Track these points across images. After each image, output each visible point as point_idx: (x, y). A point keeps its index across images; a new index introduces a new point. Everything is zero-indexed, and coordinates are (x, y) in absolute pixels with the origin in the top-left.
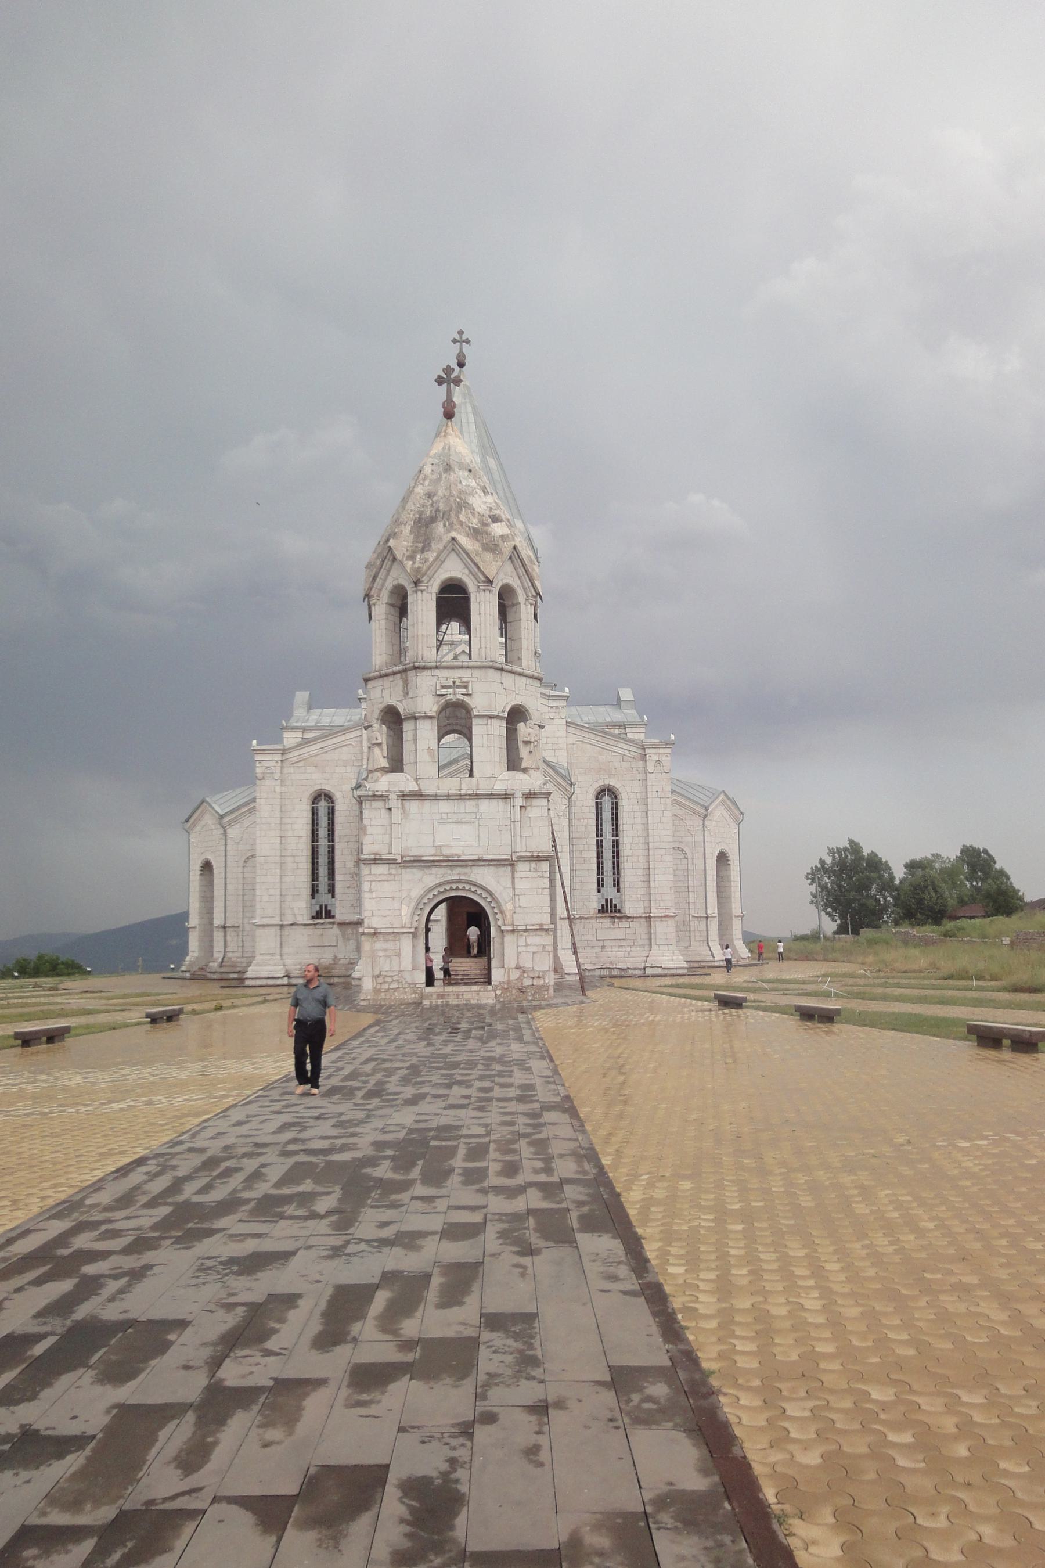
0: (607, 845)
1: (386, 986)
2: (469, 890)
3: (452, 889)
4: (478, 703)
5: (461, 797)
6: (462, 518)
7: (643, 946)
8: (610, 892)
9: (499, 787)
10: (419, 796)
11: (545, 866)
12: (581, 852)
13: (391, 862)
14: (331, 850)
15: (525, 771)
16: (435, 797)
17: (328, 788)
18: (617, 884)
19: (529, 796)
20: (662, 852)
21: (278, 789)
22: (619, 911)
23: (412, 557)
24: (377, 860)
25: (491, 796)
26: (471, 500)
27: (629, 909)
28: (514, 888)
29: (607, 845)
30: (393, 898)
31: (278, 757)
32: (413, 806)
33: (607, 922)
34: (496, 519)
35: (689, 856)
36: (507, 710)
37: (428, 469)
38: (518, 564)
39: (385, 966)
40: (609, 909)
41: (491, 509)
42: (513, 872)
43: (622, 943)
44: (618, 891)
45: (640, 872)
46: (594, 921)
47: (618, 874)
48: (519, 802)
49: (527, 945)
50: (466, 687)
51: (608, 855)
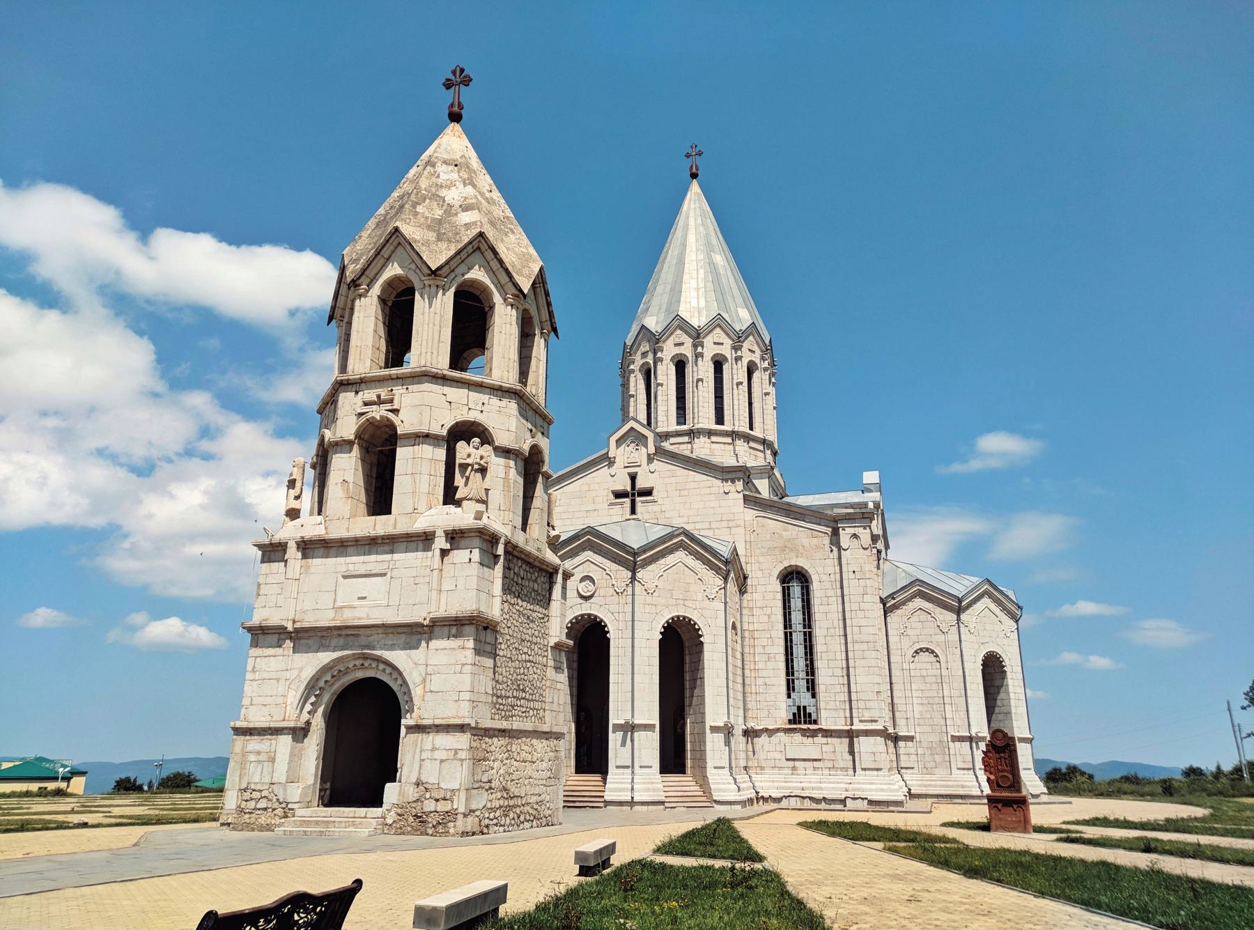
0: (798, 638)
1: (252, 804)
7: (846, 769)
8: (804, 698)
12: (764, 647)
15: (458, 503)
18: (812, 687)
20: (865, 646)
22: (815, 722)
23: (356, 261)
26: (443, 192)
29: (798, 638)
30: (278, 680)
33: (797, 737)
34: (466, 208)
35: (942, 658)
36: (447, 426)
38: (489, 255)
39: (257, 776)
40: (802, 719)
41: (466, 198)
43: (816, 764)
44: (814, 696)
45: (839, 672)
47: (813, 674)
48: (440, 543)
49: (434, 749)
50: (391, 401)
51: (799, 651)
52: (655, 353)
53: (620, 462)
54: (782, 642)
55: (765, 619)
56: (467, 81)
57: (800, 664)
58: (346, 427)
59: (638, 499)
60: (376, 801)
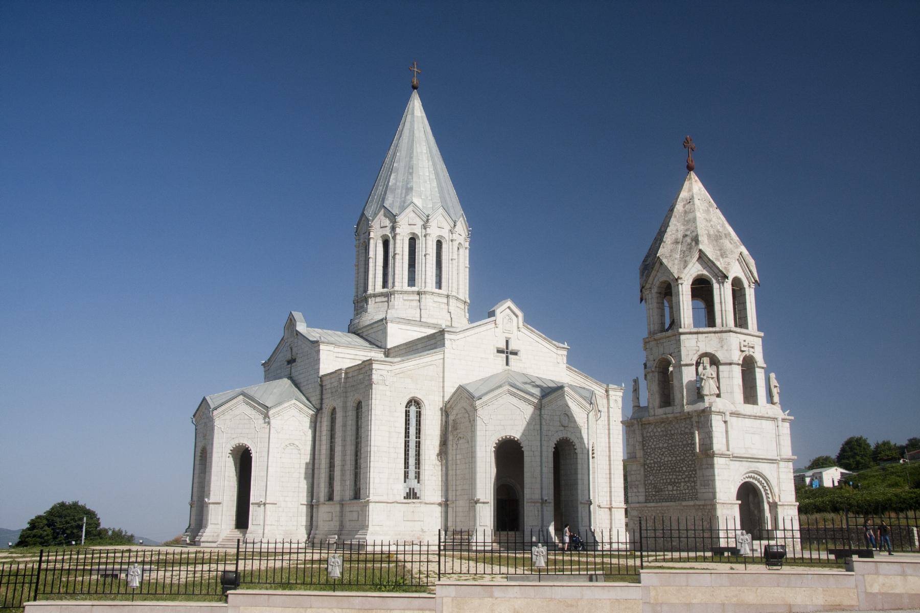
2: (756, 479)
3: (750, 477)
5: (756, 417)
9: (771, 414)
11: (791, 464)
14: (418, 445)
16: (745, 416)
17: (419, 396)
19: (784, 420)
21: (388, 393)
23: (719, 260)
24: (722, 455)
28: (779, 478)
31: (388, 368)
37: (697, 202)
42: (778, 467)
52: (425, 227)
53: (500, 326)
59: (511, 356)
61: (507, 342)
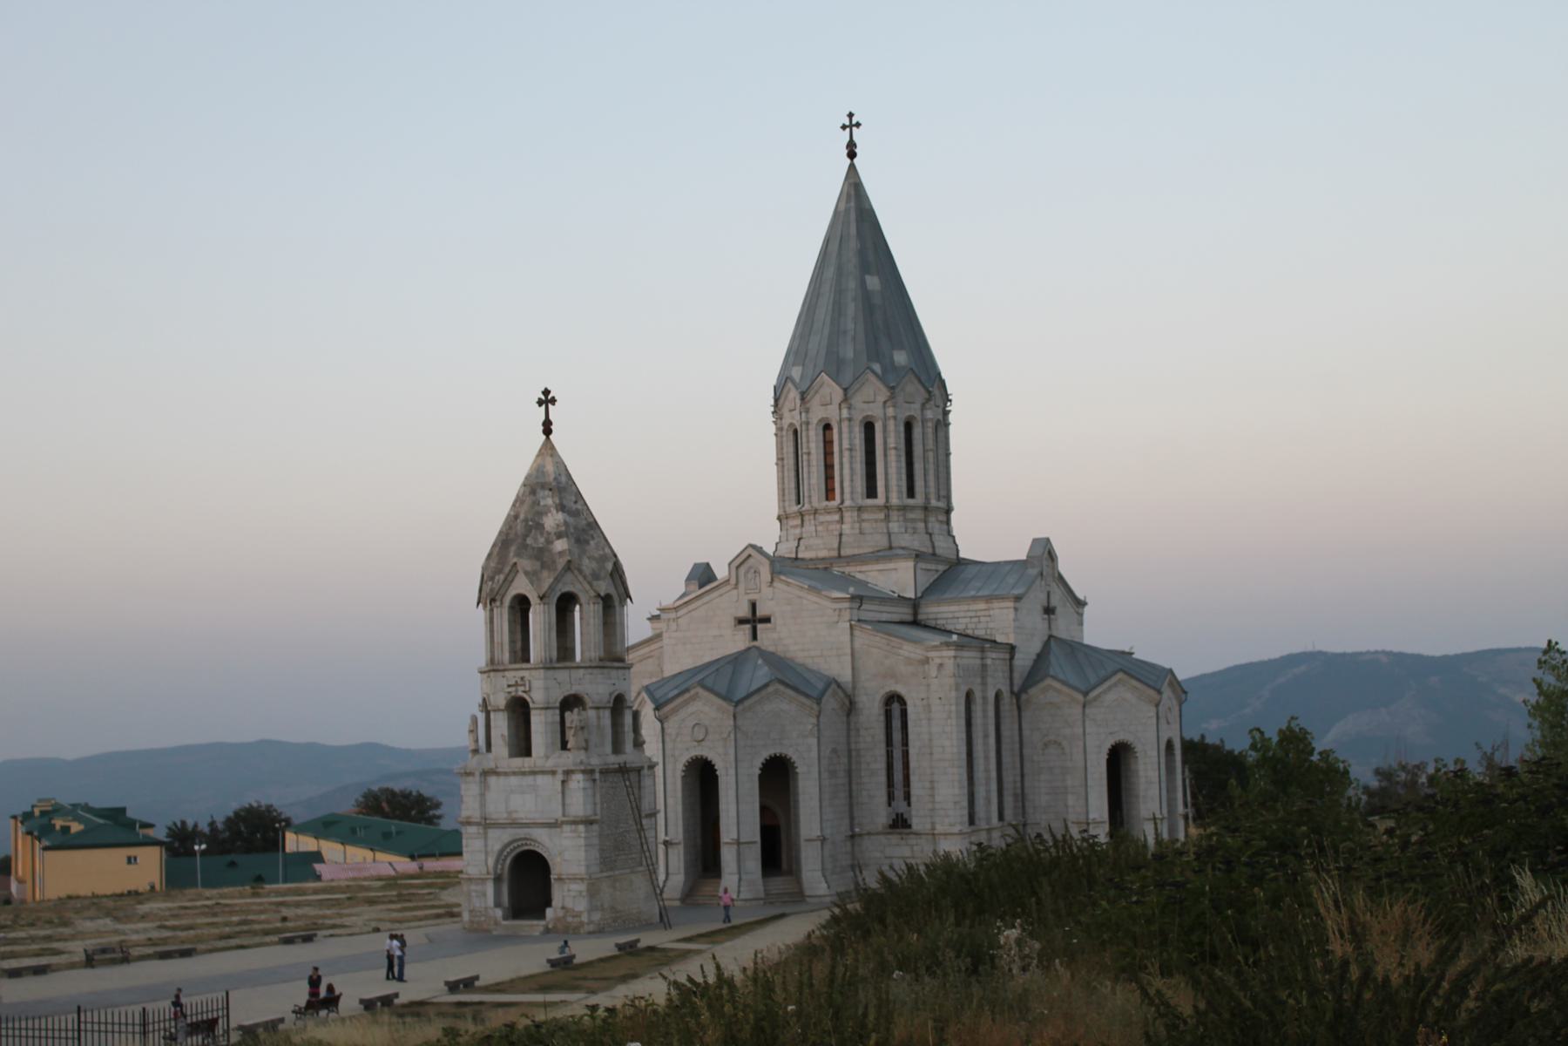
0: (897, 754)
4: (537, 697)
6: (529, 541)
8: (900, 805)
9: (550, 764)
10: (494, 772)
13: (478, 824)
16: (506, 774)
18: (907, 797)
19: (568, 773)
25: (543, 772)
27: (917, 823)
29: (897, 754)
32: (492, 780)
33: (894, 839)
34: (559, 536)
39: (477, 903)
45: (927, 785)
46: (882, 838)
48: (560, 777)
54: (884, 759)
55: (869, 739)
56: (553, 401)
57: (898, 776)
58: (500, 700)
59: (759, 626)
60: (542, 916)
61: (754, 606)
